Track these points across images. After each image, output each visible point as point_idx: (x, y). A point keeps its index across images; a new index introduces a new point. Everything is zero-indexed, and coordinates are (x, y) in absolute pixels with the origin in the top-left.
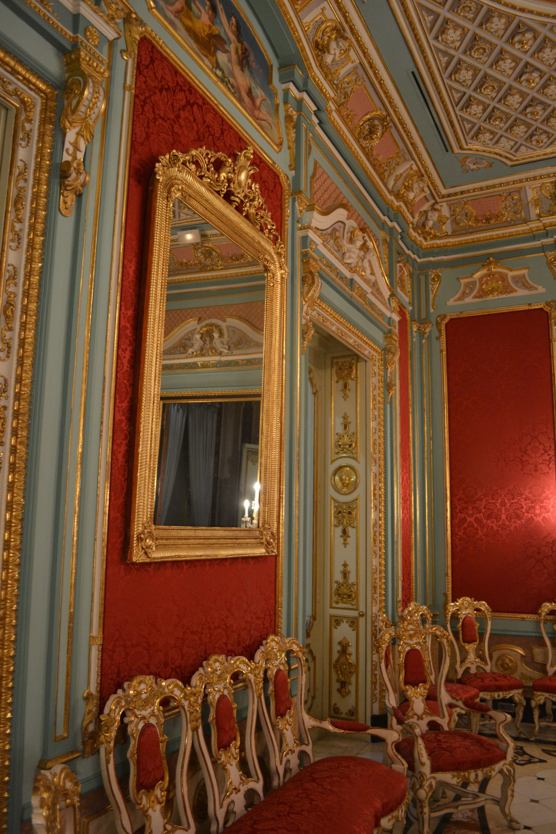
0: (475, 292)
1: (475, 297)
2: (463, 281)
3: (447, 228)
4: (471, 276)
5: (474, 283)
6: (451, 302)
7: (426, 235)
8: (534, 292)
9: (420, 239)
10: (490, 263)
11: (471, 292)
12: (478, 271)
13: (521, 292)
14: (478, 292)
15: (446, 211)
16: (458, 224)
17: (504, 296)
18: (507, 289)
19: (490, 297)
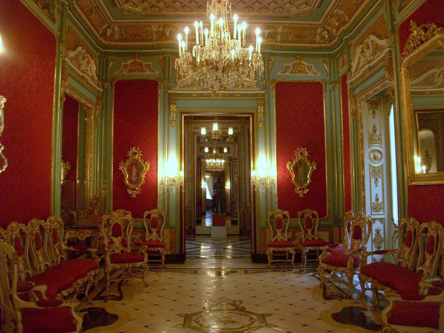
0: (127, 70)
1: (128, 72)
2: (122, 64)
3: (117, 36)
4: (127, 61)
5: (127, 65)
6: (116, 73)
7: (106, 39)
8: (154, 73)
9: (104, 41)
10: (135, 57)
11: (126, 69)
12: (130, 60)
13: (148, 73)
14: (129, 70)
15: (116, 28)
16: (122, 36)
17: (140, 73)
18: (142, 70)
19: (134, 73)
